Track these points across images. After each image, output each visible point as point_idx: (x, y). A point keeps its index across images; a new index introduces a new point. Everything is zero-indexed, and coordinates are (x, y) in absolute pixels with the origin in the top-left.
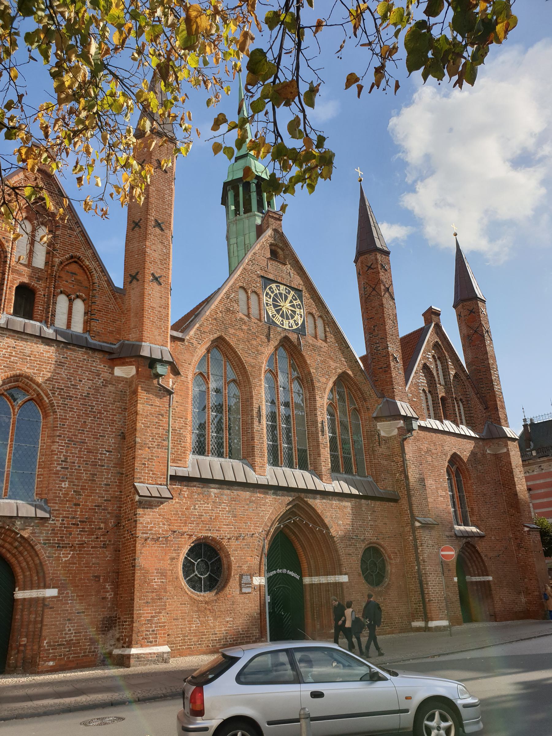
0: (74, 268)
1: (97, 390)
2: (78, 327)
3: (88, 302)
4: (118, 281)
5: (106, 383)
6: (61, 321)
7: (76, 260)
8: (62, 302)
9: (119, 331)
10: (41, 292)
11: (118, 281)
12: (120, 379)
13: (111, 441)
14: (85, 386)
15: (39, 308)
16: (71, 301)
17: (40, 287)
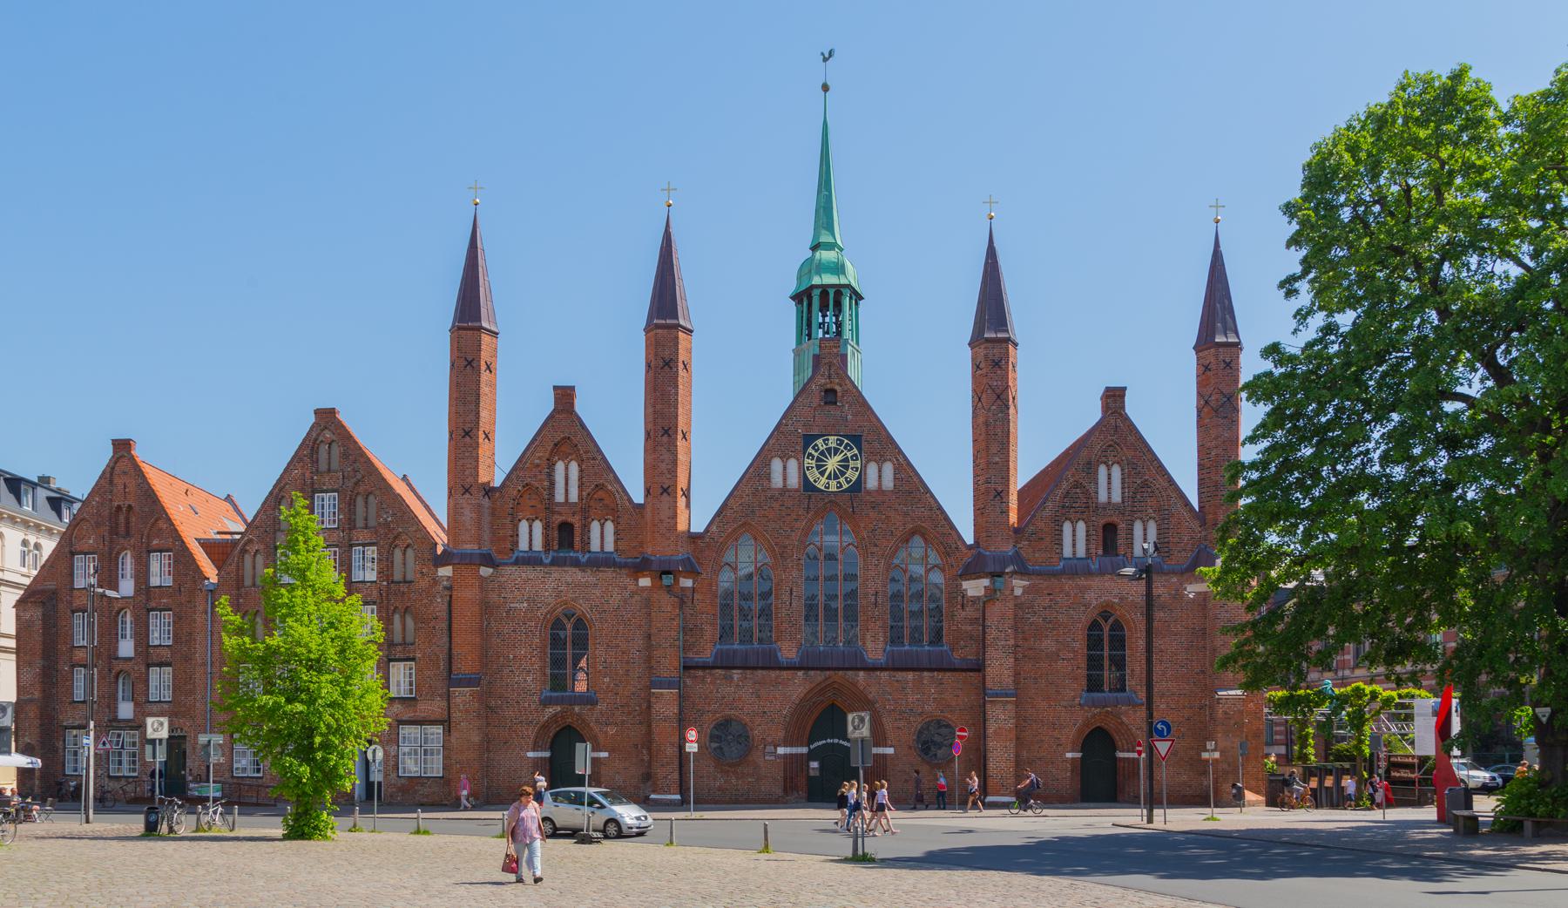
0: (601, 494)
1: (625, 601)
2: (610, 547)
3: (616, 523)
4: (638, 496)
5: (633, 594)
6: (595, 546)
7: (599, 487)
8: (595, 527)
9: (641, 544)
10: (577, 525)
11: (638, 496)
12: (644, 589)
13: (640, 642)
14: (616, 599)
15: (577, 539)
16: (602, 526)
17: (575, 521)
